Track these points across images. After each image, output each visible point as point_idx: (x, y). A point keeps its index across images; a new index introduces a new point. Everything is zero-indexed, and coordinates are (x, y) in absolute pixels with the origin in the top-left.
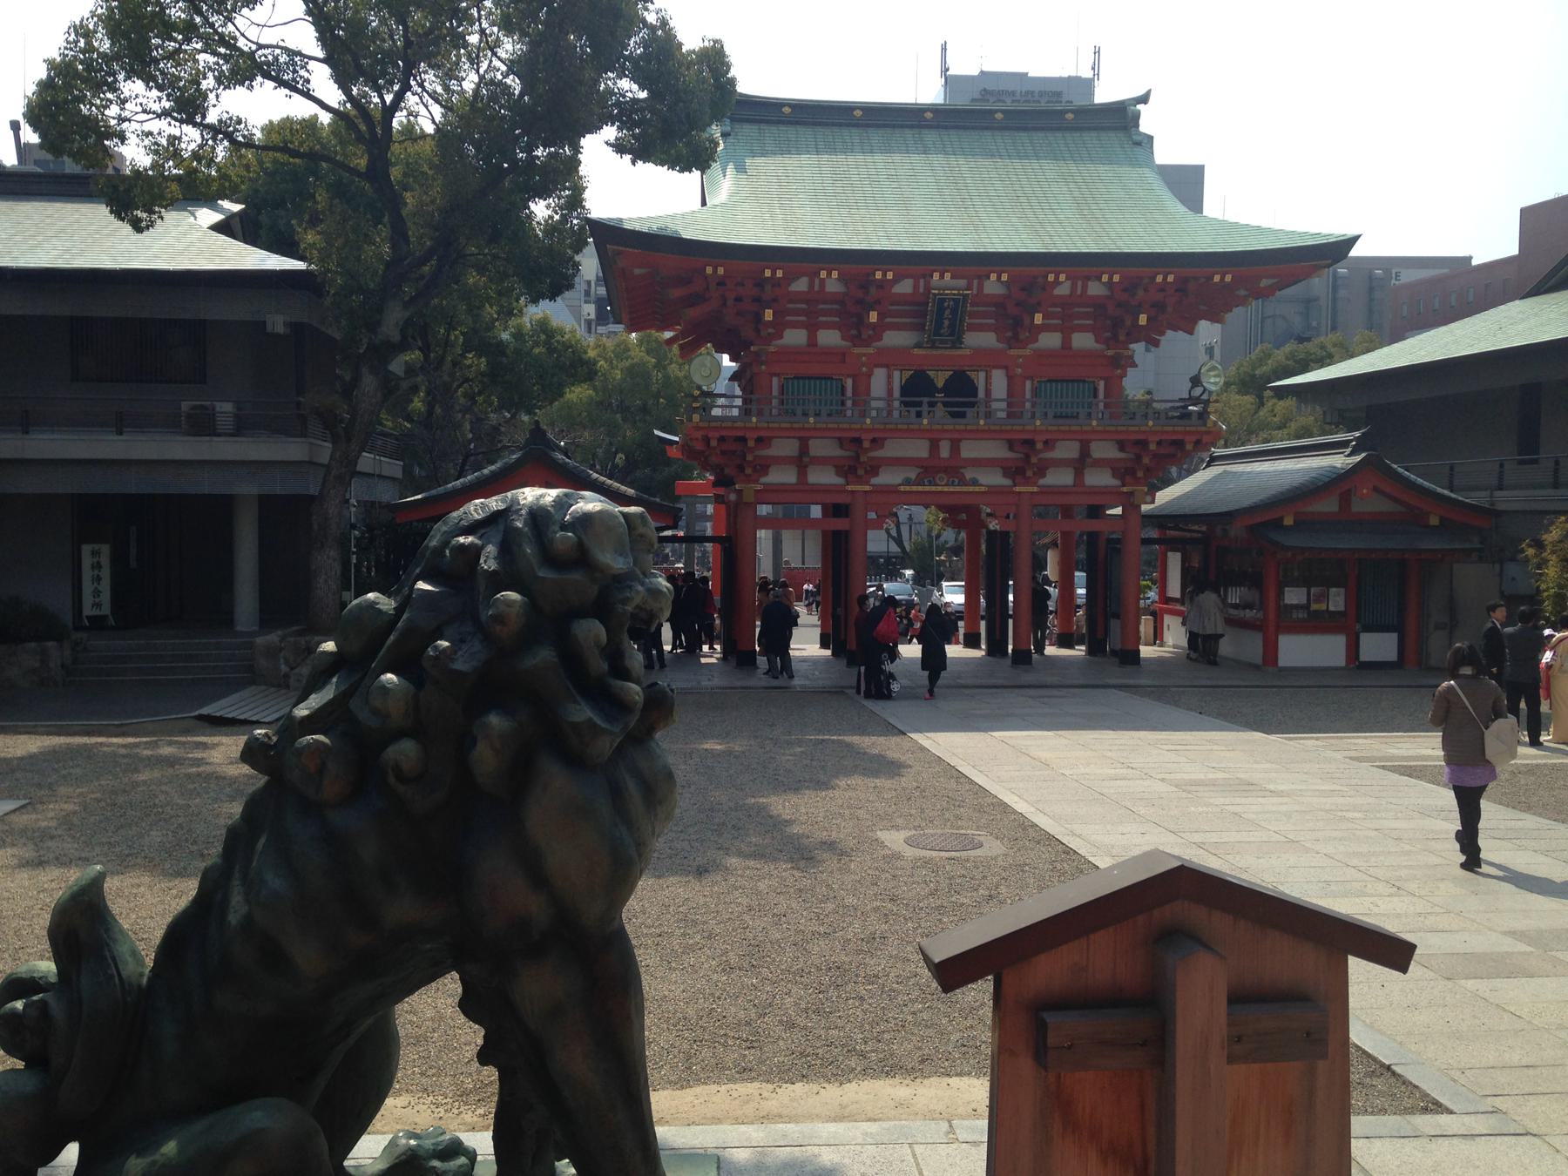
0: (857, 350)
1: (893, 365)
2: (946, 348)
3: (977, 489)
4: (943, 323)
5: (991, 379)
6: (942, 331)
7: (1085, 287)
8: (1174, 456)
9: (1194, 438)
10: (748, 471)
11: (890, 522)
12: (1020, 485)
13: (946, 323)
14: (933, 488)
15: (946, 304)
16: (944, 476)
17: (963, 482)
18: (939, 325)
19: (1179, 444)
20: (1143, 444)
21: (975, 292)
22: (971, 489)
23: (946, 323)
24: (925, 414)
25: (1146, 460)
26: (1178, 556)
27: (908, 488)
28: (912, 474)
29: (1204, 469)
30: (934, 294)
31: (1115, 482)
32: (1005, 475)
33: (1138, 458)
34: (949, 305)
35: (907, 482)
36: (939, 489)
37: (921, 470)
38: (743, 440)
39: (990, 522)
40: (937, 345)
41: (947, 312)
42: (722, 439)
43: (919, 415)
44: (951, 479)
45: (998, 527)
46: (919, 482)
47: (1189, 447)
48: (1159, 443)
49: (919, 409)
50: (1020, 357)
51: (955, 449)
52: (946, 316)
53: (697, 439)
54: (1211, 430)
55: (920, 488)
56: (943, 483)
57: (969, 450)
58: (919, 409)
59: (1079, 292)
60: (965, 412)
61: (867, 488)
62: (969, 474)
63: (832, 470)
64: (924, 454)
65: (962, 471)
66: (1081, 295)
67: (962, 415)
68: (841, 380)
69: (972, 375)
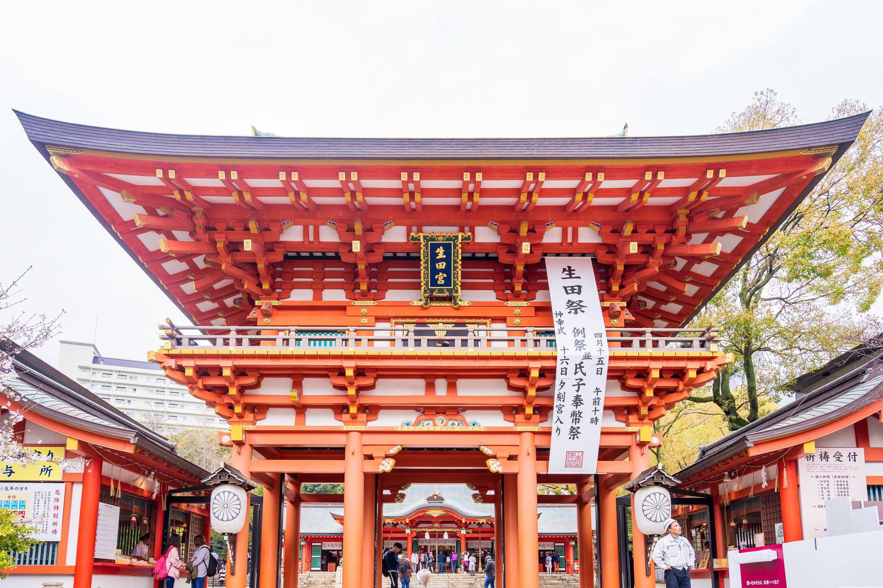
0: (357, 303)
3: (476, 429)
14: (431, 429)
19: (679, 374)
20: (642, 374)
22: (470, 429)
27: (405, 429)
28: (412, 417)
36: (438, 429)
37: (418, 414)
38: (219, 370)
42: (202, 372)
44: (452, 422)
46: (417, 423)
47: (692, 374)
48: (662, 371)
51: (452, 386)
53: (170, 368)
57: (468, 390)
62: (470, 417)
64: (421, 392)
67: (452, 343)
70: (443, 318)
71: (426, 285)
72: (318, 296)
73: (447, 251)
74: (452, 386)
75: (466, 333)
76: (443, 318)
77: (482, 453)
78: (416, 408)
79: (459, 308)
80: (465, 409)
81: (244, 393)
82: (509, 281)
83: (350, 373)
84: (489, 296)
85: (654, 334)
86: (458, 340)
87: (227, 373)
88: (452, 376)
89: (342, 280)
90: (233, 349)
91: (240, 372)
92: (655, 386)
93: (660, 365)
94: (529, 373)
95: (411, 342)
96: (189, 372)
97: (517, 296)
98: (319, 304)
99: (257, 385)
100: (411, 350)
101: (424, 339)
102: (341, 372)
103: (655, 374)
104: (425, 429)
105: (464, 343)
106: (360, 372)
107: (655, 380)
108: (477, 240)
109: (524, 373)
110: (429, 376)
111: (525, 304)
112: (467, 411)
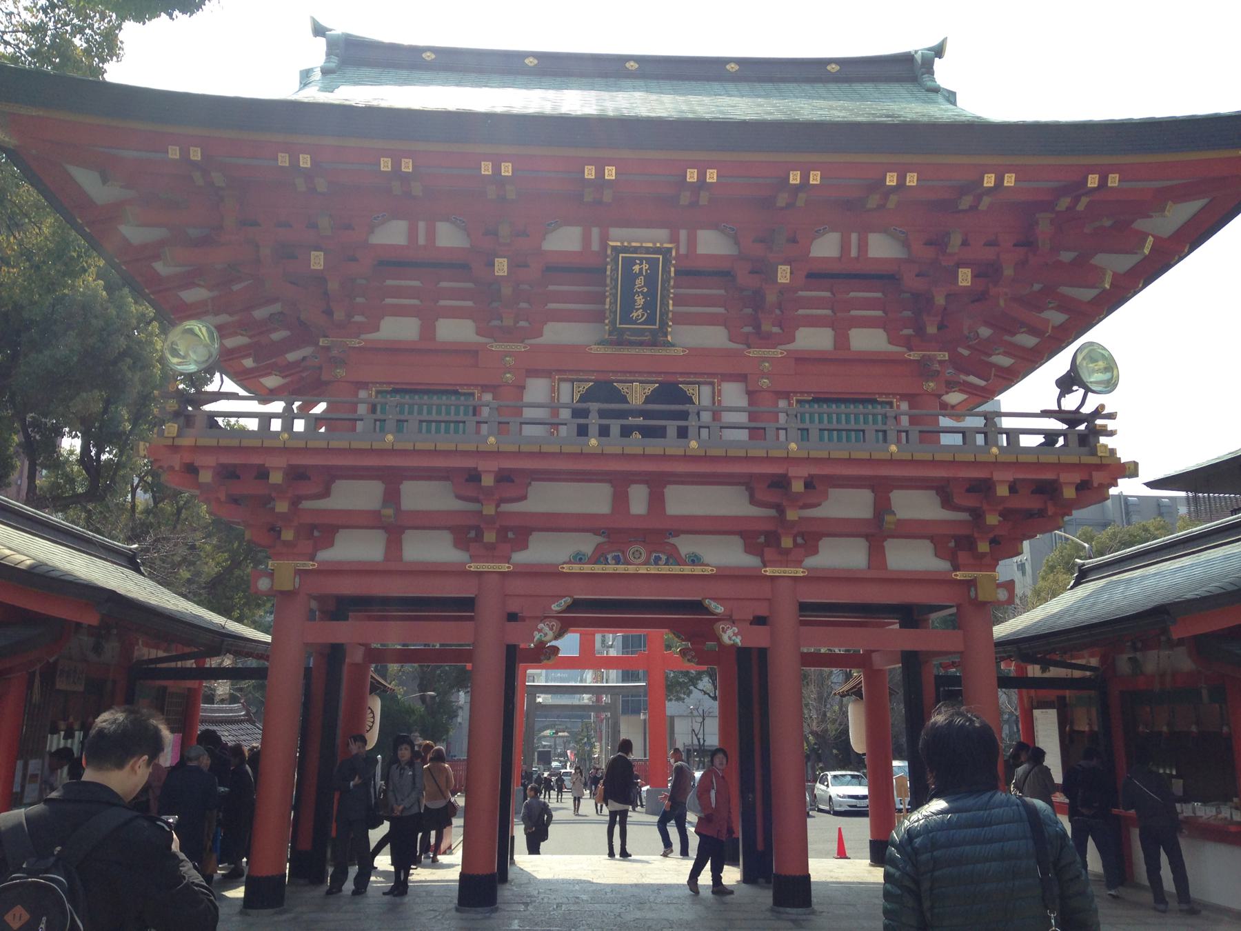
0: (496, 347)
1: (559, 371)
2: (641, 344)
3: (698, 570)
4: (635, 301)
5: (719, 395)
6: (635, 314)
7: (863, 246)
8: (1042, 513)
9: (1077, 478)
10: (288, 535)
11: (546, 629)
12: (774, 563)
13: (640, 300)
14: (621, 569)
15: (636, 268)
16: (643, 551)
17: (677, 560)
18: (629, 305)
21: (683, 251)
22: (687, 570)
23: (640, 300)
24: (593, 430)
25: (992, 519)
26: (1052, 714)
27: (576, 568)
28: (587, 544)
29: (1072, 588)
30: (614, 248)
31: (942, 565)
32: (750, 549)
33: (977, 515)
34: (641, 270)
35: (579, 558)
36: (631, 569)
37: (600, 539)
38: (262, 473)
39: (724, 631)
40: (626, 337)
41: (640, 282)
42: (229, 474)
43: (583, 431)
45: (738, 640)
47: (1069, 493)
48: (1013, 488)
49: (582, 421)
50: (765, 359)
51: (657, 500)
52: (636, 289)
54: (1104, 462)
55: (598, 569)
56: (639, 561)
58: (582, 421)
59: (854, 253)
60: (665, 427)
61: (505, 567)
62: (685, 545)
63: (447, 537)
65: (673, 540)
66: (857, 259)
67: (660, 433)
68: (473, 394)
69: (690, 390)
70: (640, 373)
71: (613, 323)
72: (428, 331)
74: (657, 500)
75: (684, 415)
76: (640, 373)
77: (707, 611)
78: (596, 532)
80: (677, 533)
81: (300, 506)
82: (749, 311)
83: (488, 481)
84: (714, 337)
86: (672, 426)
87: (276, 478)
88: (657, 484)
89: (470, 303)
91: (297, 475)
92: (1000, 508)
93: (1009, 476)
94: (789, 484)
95: (593, 430)
96: (206, 477)
97: (767, 340)
99: (326, 494)
101: (615, 426)
102: (474, 477)
103: (1002, 491)
104: (610, 568)
105: (683, 433)
106: (504, 477)
107: (1003, 498)
108: (701, 250)
110: (620, 483)
111: (778, 352)
112: (682, 536)
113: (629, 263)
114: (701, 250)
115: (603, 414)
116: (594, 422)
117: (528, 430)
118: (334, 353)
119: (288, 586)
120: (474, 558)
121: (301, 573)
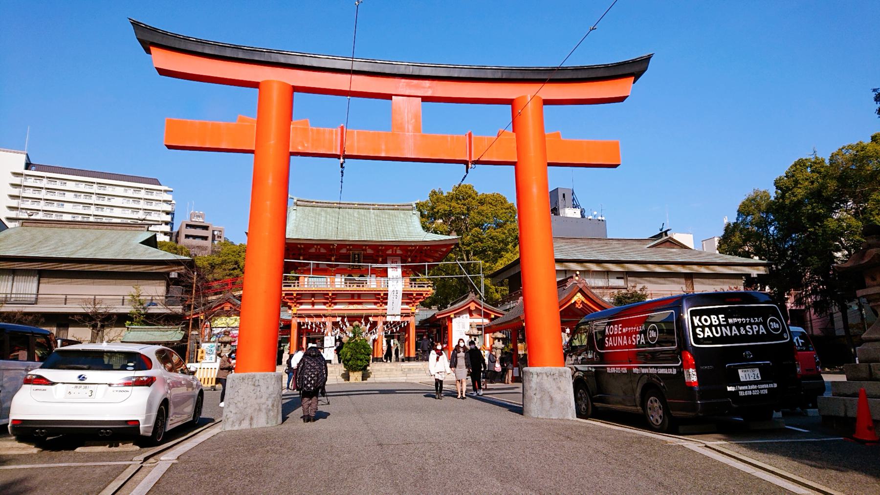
14: (353, 308)
59: (394, 253)
67: (359, 286)
73: (358, 255)
79: (361, 271)
85: (415, 284)
86: (361, 285)
90: (296, 288)
95: (348, 286)
98: (318, 269)
100: (348, 289)
101: (352, 285)
104: (351, 308)
109: (379, 294)
113: (355, 255)
114: (368, 252)
115: (349, 283)
116: (348, 284)
117: (337, 286)
118: (302, 271)
119: (296, 312)
120: (327, 307)
121: (297, 310)
